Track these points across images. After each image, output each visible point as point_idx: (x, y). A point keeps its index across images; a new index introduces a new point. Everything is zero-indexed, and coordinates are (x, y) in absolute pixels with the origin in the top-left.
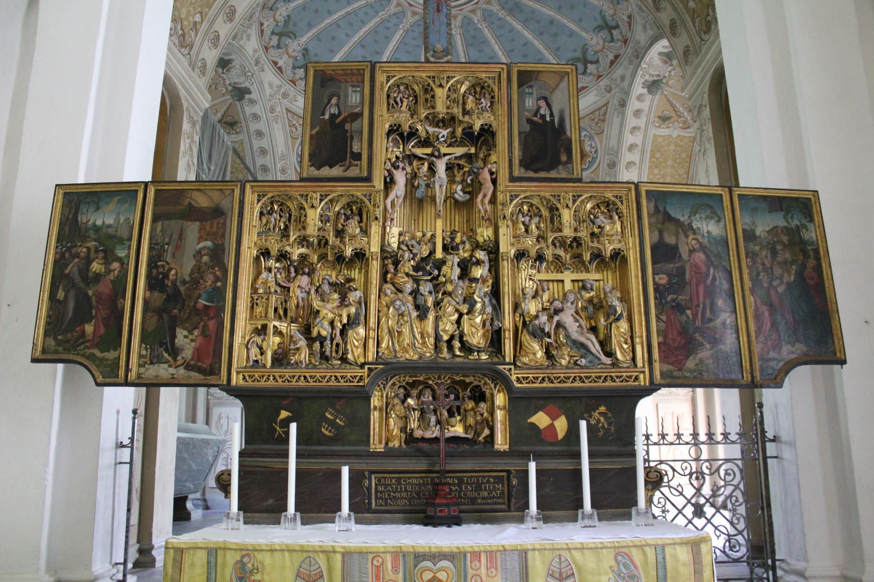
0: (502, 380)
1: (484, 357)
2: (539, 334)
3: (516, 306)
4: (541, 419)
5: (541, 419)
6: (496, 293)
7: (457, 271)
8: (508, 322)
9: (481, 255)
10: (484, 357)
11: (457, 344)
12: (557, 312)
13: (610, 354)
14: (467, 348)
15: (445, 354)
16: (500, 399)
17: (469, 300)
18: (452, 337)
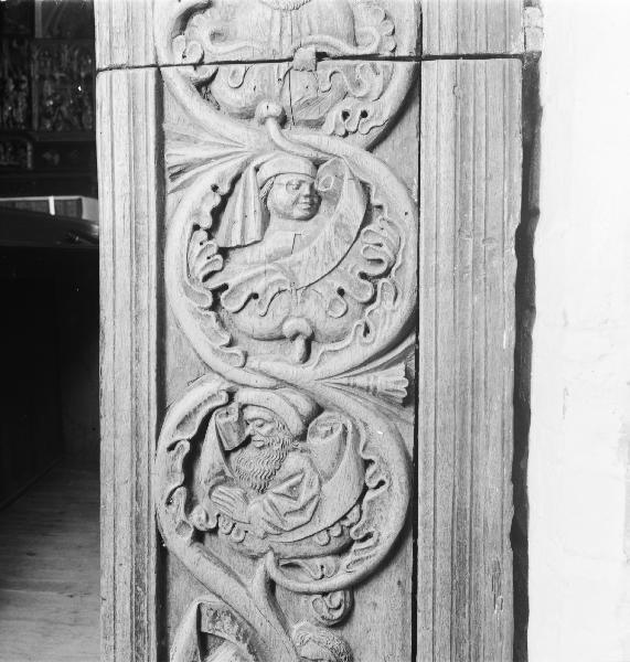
0: (31, 139)
1: (23, 127)
2: (48, 116)
3: (40, 104)
4: (47, 156)
5: (47, 156)
6: (29, 99)
7: (12, 87)
8: (36, 110)
9: (24, 78)
10: (23, 127)
11: (11, 122)
12: (60, 105)
13: (82, 125)
14: (15, 123)
15: (6, 126)
16: (29, 147)
17: (16, 102)
18: (8, 118)
